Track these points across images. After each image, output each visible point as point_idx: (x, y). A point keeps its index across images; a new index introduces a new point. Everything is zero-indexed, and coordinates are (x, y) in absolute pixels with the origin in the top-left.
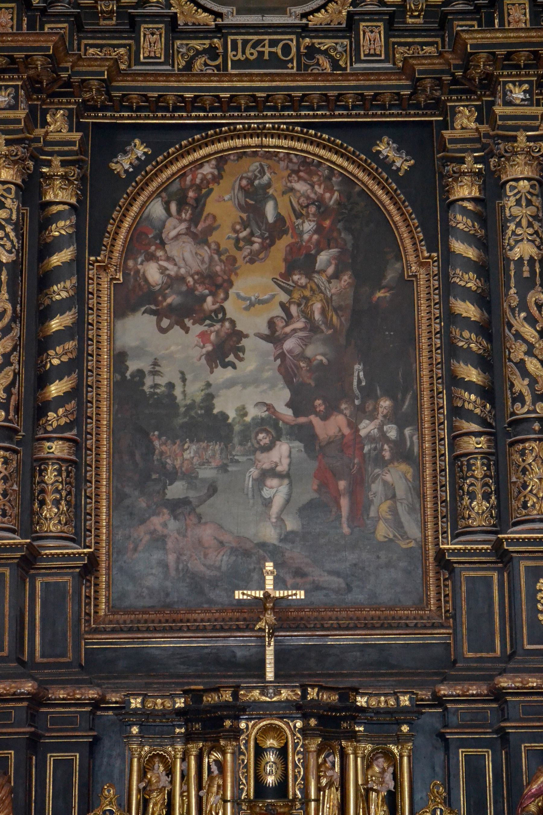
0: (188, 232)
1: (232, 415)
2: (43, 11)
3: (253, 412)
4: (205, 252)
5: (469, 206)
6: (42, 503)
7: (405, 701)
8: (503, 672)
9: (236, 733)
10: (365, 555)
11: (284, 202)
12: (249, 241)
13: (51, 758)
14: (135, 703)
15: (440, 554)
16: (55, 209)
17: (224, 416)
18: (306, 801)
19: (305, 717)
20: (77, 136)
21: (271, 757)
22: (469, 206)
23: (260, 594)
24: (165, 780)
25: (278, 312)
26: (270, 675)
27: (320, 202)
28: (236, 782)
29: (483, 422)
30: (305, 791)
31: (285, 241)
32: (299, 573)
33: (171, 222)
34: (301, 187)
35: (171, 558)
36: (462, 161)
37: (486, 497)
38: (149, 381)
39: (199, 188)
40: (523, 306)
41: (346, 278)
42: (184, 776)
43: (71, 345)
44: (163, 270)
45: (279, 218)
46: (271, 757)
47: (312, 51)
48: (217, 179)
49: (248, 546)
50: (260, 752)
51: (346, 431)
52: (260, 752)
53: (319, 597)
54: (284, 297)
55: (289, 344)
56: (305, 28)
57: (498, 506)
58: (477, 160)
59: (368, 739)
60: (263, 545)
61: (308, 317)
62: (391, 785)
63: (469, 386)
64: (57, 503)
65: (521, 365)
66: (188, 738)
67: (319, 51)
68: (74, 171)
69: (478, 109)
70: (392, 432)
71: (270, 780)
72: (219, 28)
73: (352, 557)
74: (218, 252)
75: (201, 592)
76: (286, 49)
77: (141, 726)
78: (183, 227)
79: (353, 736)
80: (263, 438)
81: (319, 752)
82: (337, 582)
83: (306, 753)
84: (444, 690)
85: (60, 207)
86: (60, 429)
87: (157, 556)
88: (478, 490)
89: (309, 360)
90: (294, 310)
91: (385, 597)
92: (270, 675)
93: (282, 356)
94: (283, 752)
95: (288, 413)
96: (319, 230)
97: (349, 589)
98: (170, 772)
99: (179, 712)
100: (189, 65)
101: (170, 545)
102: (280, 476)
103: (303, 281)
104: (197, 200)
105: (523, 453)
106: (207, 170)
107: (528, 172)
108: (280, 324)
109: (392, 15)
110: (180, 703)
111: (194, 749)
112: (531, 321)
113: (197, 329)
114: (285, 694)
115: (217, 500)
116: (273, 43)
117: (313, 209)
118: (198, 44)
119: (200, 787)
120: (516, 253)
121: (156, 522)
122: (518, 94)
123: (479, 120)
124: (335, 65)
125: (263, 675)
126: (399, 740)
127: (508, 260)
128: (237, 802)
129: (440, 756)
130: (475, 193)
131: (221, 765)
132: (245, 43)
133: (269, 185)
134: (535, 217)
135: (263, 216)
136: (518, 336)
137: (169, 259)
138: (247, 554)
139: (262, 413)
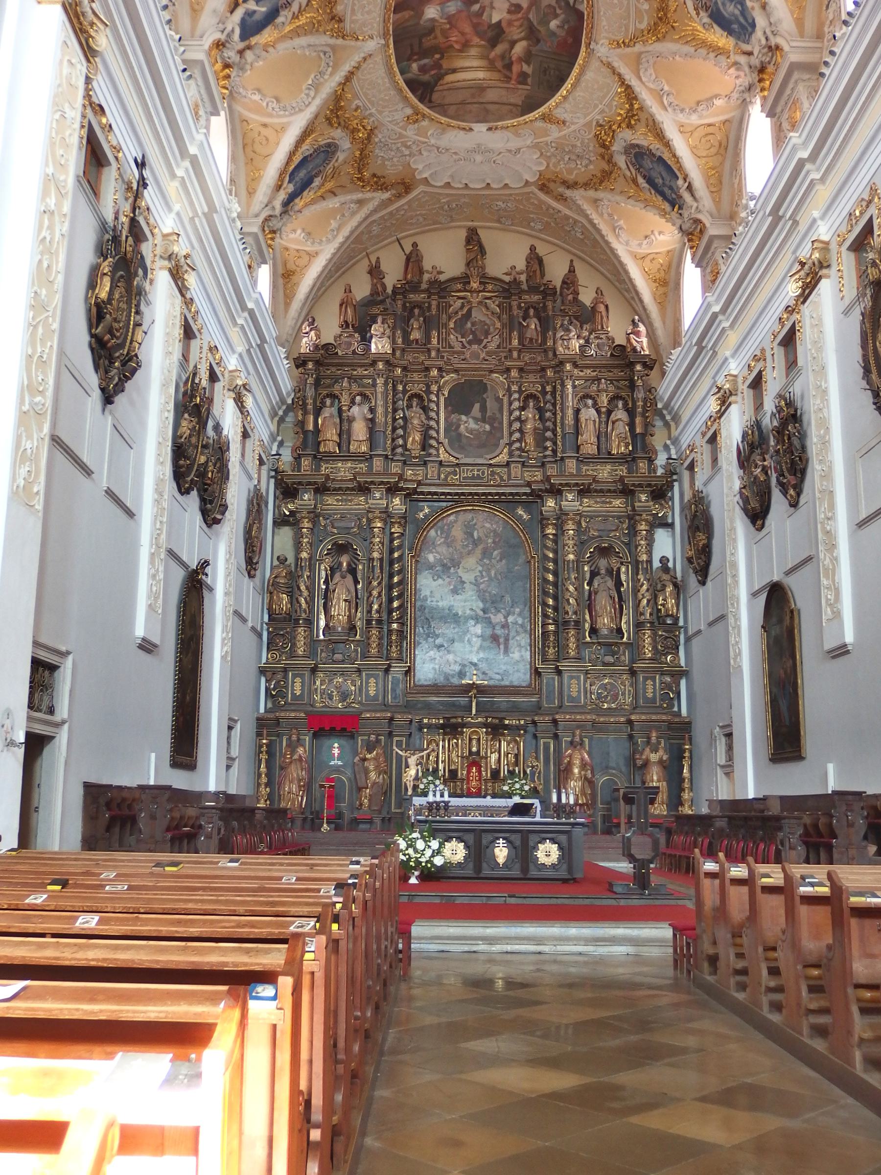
0: (444, 542)
1: (460, 613)
2: (392, 459)
3: (468, 612)
4: (451, 550)
5: (551, 537)
6: (391, 646)
7: (522, 722)
8: (557, 713)
9: (462, 733)
10: (509, 667)
11: (480, 530)
12: (467, 546)
13: (395, 739)
14: (425, 721)
15: (536, 669)
16: (396, 535)
17: (457, 614)
18: (486, 758)
19: (486, 728)
20: (404, 507)
21: (474, 742)
22: (551, 537)
23: (471, 682)
24: (436, 748)
25: (478, 574)
26: (474, 712)
27: (495, 531)
28: (462, 750)
29: (554, 620)
30: (486, 753)
31: (480, 547)
32: (484, 673)
33: (438, 538)
34: (488, 525)
35: (437, 667)
36: (548, 519)
37: (554, 648)
38: (429, 600)
39: (449, 525)
40: (569, 578)
41: (504, 561)
42: (443, 747)
43: (401, 587)
44: (435, 557)
45: (479, 538)
46: (474, 742)
47: (493, 473)
48: (456, 521)
49: (466, 663)
50: (471, 740)
51: (503, 620)
52: (471, 740)
53: (492, 683)
54: (480, 568)
55: (482, 586)
56: (490, 465)
57: (558, 652)
58: (555, 519)
59: (508, 735)
60: (471, 663)
61: (489, 575)
62: (516, 752)
63: (548, 606)
64: (396, 647)
65: (568, 600)
66: (445, 734)
67: (495, 473)
68: (403, 522)
69: (556, 499)
70: (520, 621)
71: (474, 749)
72: (458, 464)
73: (504, 668)
74: (456, 550)
75: (448, 680)
76: (483, 473)
77: (428, 728)
78: (443, 540)
79: (503, 735)
80: (472, 622)
81: (492, 740)
82: (498, 677)
83: (487, 741)
84: (536, 718)
85: (396, 535)
86: (397, 619)
87: (432, 666)
88: (551, 644)
89: (490, 593)
90: (484, 573)
91: (516, 683)
92: (474, 712)
93: (479, 591)
94: (479, 740)
95: (481, 613)
96: (494, 542)
97: (503, 680)
98: (438, 745)
99: (441, 724)
100: (446, 477)
101: (437, 661)
102: (478, 637)
103: (488, 562)
104: (448, 529)
105: (567, 633)
106: (452, 518)
107: (573, 527)
108: (479, 579)
109: (524, 462)
110: (441, 722)
111: (447, 738)
112: (573, 585)
113: (448, 580)
114: (480, 720)
115: (456, 644)
116: (478, 470)
117: (492, 534)
118: (448, 469)
119: (449, 751)
120: (567, 558)
121: (432, 653)
122: (570, 497)
123: (556, 504)
124: (501, 478)
125: (471, 711)
126: (520, 736)
127: (564, 560)
128: (462, 757)
129: (534, 742)
130: (554, 532)
131: (457, 744)
132: (468, 470)
133: (475, 524)
134: (575, 544)
135: (472, 536)
136: (567, 589)
137: (437, 552)
138: (464, 666)
139: (473, 613)
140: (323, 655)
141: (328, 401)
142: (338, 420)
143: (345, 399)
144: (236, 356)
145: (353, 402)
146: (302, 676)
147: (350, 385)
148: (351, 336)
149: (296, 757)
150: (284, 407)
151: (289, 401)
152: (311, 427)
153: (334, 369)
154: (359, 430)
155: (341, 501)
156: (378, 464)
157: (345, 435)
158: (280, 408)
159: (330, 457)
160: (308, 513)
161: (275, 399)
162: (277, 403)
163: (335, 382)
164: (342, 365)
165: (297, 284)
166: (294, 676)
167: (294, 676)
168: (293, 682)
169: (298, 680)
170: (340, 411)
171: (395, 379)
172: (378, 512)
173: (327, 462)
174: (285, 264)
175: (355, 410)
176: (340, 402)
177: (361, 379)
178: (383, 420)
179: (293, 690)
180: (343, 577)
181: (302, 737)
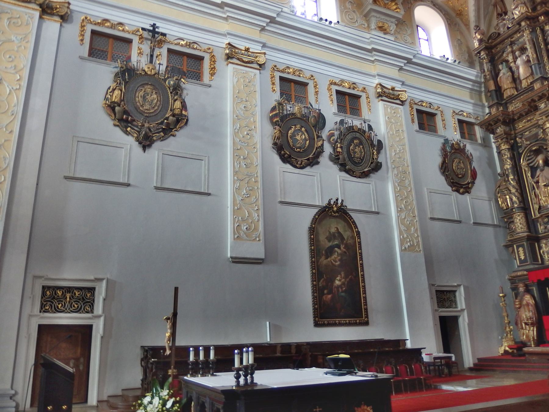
140: (542, 227)
141: (500, 67)
142: (510, 73)
143: (510, 58)
144: (377, 77)
145: (515, 59)
146: (522, 246)
147: (512, 48)
148: (504, 20)
149: (524, 302)
150: (483, 85)
151: (483, 80)
152: (492, 87)
153: (501, 46)
154: (522, 71)
155: (528, 121)
156: (537, 86)
157: (515, 79)
158: (480, 87)
159: (512, 98)
160: (502, 140)
161: (469, 85)
162: (472, 85)
163: (503, 53)
164: (503, 41)
165: (468, 15)
166: (518, 247)
167: (518, 247)
168: (518, 252)
169: (521, 249)
170: (510, 69)
171: (541, 25)
172: (544, 117)
173: (511, 103)
174: (454, 9)
175: (519, 61)
176: (507, 61)
177: (518, 40)
178: (535, 56)
179: (519, 256)
180: (542, 170)
181: (530, 288)
